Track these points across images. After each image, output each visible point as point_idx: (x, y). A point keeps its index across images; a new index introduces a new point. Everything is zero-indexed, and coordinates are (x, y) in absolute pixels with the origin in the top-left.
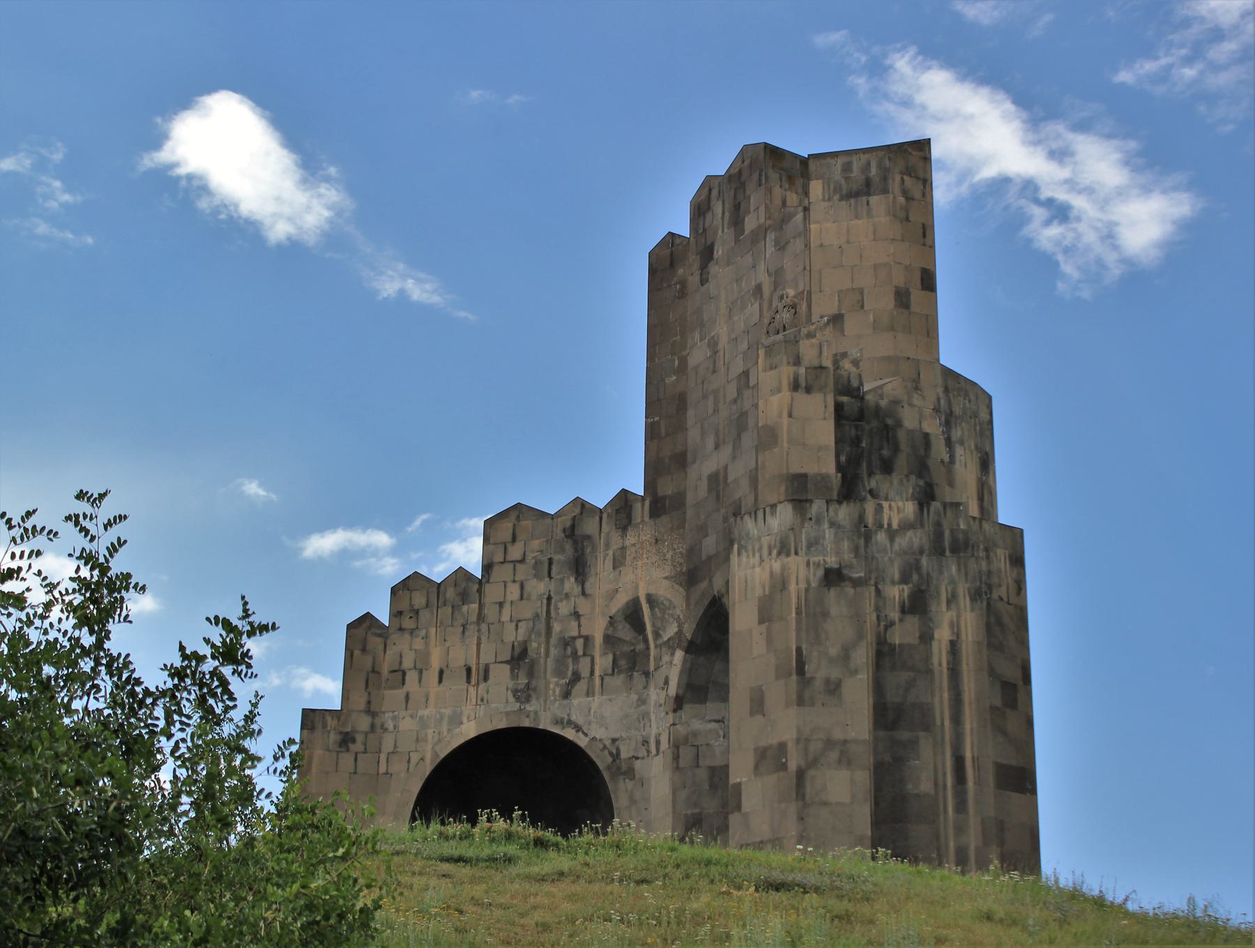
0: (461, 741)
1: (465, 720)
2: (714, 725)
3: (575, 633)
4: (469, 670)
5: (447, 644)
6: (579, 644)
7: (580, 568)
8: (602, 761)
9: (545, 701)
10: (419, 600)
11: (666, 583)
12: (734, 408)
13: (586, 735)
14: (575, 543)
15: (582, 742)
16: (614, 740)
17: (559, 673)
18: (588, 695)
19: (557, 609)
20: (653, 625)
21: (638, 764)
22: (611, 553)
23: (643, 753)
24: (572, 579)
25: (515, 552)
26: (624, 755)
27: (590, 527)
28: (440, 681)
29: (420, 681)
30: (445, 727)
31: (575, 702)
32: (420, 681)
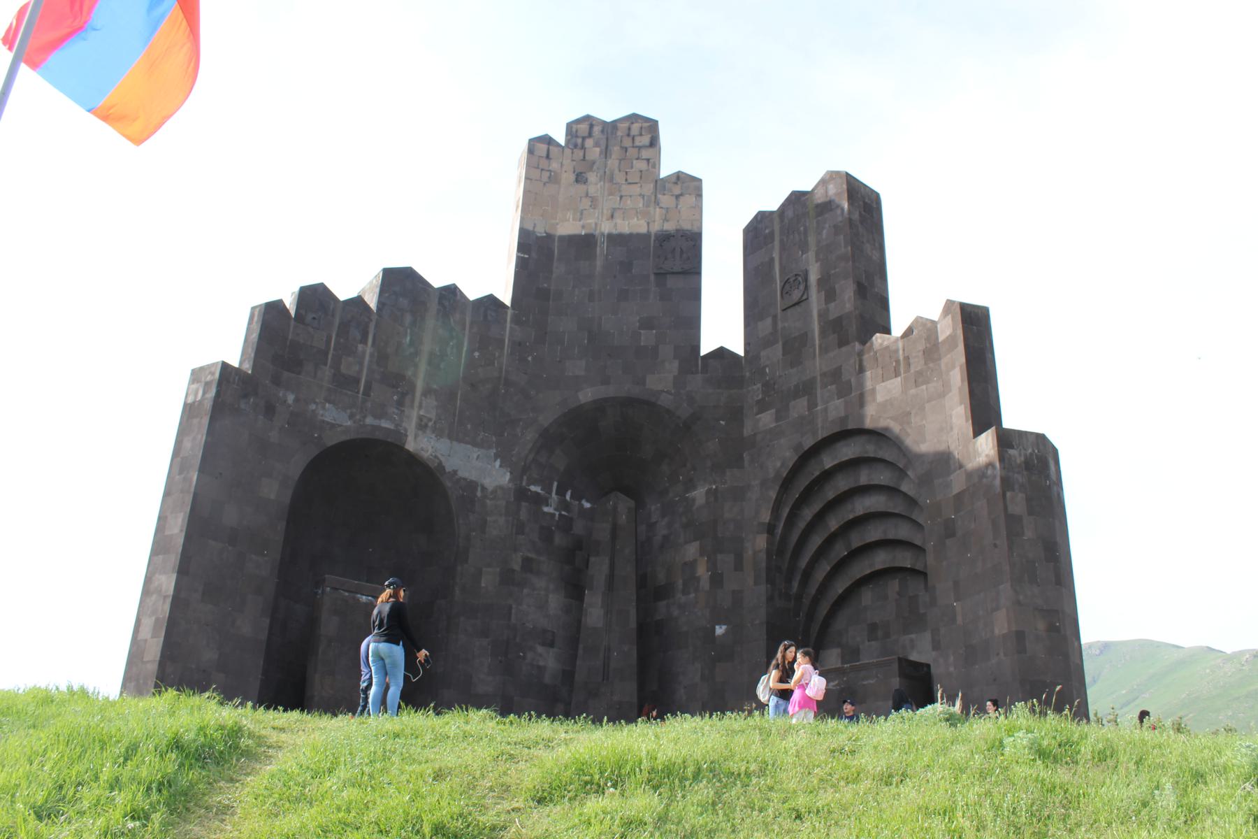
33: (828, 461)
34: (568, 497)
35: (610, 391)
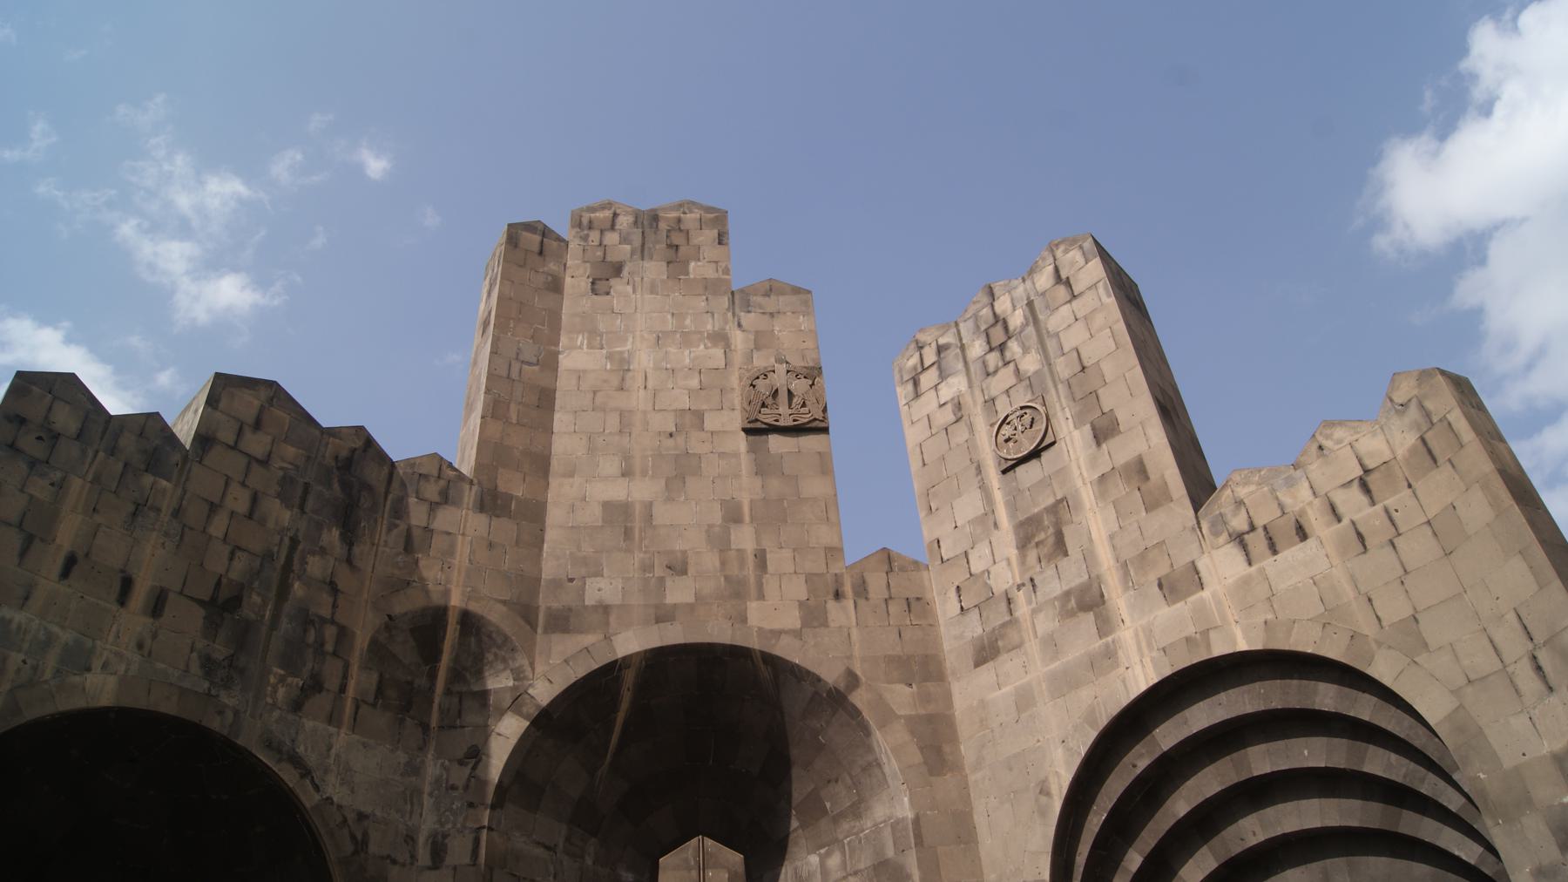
0: (78, 703)
1: (97, 664)
2: (539, 851)
3: (325, 612)
4: (127, 585)
5: (98, 518)
6: (330, 632)
7: (348, 520)
10: (65, 420)
11: (504, 609)
12: (670, 442)
13: (317, 788)
14: (345, 485)
15: (309, 799)
16: (361, 817)
17: (290, 663)
18: (330, 720)
19: (304, 562)
20: (456, 659)
21: (394, 871)
22: (403, 527)
24: (336, 533)
25: (257, 444)
26: (373, 848)
27: (374, 475)
28: (65, 573)
29: (23, 553)
30: (51, 660)
31: (309, 724)
32: (23, 553)
33: (1168, 735)
34: (589, 861)
35: (674, 635)
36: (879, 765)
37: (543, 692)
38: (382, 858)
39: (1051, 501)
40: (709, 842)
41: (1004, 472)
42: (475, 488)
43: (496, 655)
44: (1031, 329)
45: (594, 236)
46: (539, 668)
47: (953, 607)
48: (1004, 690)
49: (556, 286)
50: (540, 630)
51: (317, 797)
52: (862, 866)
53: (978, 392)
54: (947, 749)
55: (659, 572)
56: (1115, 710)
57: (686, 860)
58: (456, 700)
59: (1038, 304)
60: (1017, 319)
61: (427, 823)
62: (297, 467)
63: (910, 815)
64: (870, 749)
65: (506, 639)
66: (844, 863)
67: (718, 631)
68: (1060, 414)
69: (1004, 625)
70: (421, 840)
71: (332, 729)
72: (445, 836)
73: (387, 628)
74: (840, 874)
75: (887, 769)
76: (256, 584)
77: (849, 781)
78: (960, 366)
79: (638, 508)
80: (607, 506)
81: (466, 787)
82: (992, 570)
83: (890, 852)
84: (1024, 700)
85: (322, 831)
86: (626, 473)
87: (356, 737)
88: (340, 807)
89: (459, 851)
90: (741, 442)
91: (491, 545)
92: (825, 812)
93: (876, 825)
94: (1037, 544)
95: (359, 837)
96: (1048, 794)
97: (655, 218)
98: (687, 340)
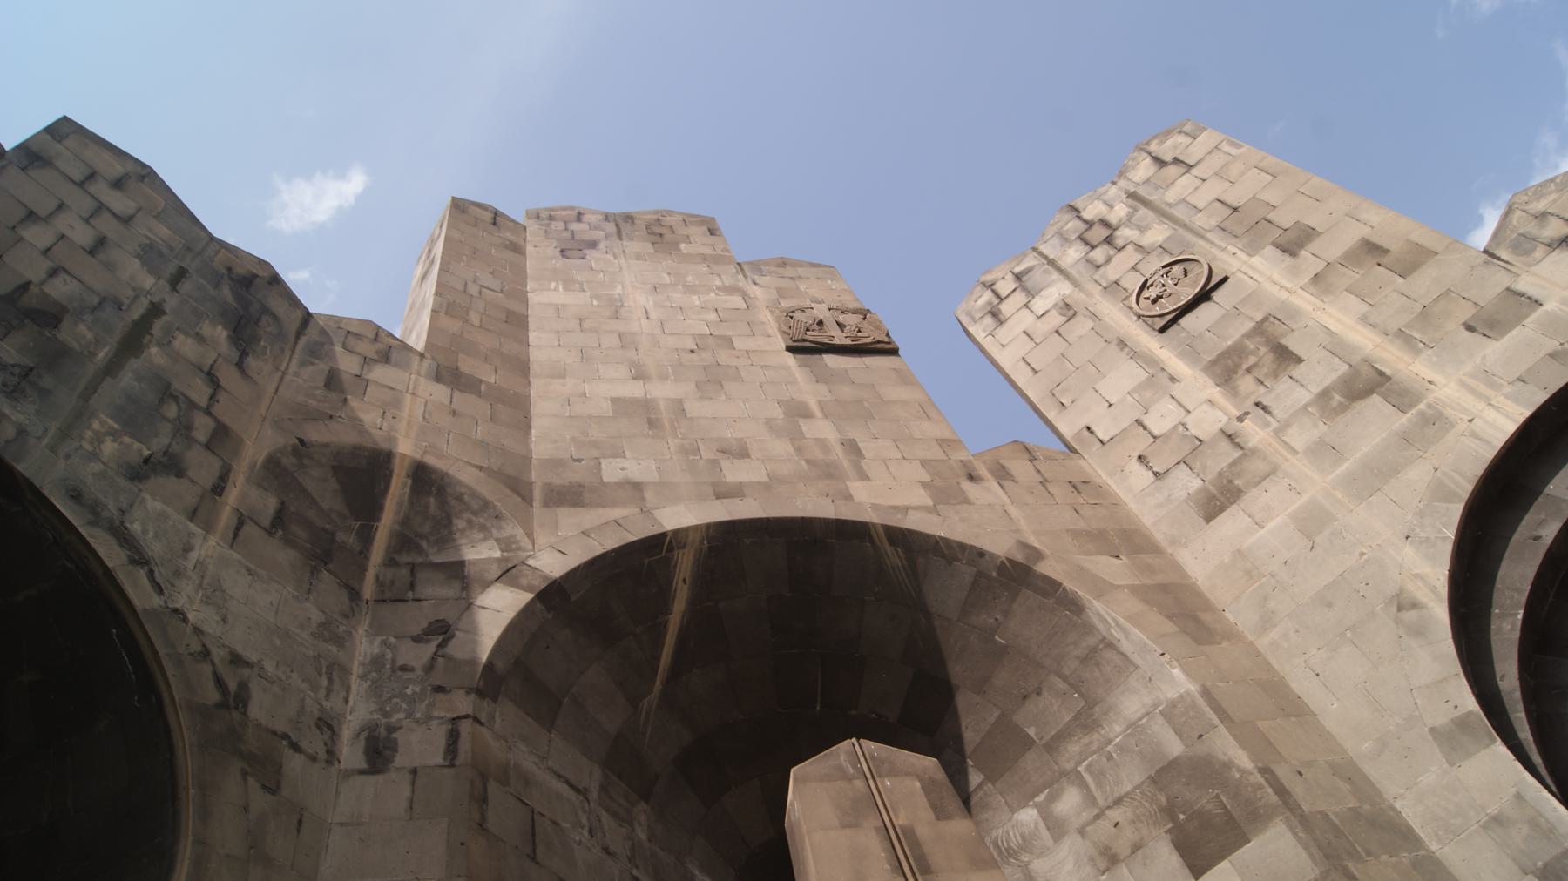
6: (202, 427)
8: (186, 689)
9: (65, 434)
13: (159, 590)
16: (236, 660)
17: (134, 418)
18: (193, 515)
20: (405, 522)
22: (323, 367)
23: (314, 742)
26: (256, 711)
34: (642, 834)
36: (1111, 646)
37: (552, 563)
38: (275, 733)
39: (1249, 325)
40: (871, 746)
41: (1162, 330)
42: (426, 363)
43: (470, 522)
44: (1143, 211)
45: (559, 225)
46: (542, 539)
47: (1140, 477)
48: (1270, 526)
49: (518, 249)
50: (536, 504)
51: (157, 601)
52: (1127, 787)
53: (1090, 286)
54: (1206, 617)
55: (706, 455)
56: (1479, 469)
57: (840, 768)
58: (405, 572)
59: (1142, 191)
60: (1120, 211)
61: (357, 711)
62: (171, 249)
63: (1193, 688)
64: (1088, 628)
65: (486, 504)
66: (1090, 799)
67: (811, 503)
68: (1220, 254)
69: (1234, 463)
70: (346, 734)
71: (192, 527)
72: (391, 729)
73: (295, 452)
74: (1086, 816)
75: (1125, 646)
76: (88, 317)
77: (1062, 685)
78: (1055, 275)
79: (662, 405)
80: (614, 401)
81: (430, 668)
82: (1189, 420)
83: (1174, 747)
84: (1312, 523)
85: (162, 652)
86: (640, 375)
87: (236, 556)
88: (197, 631)
89: (421, 745)
90: (791, 360)
91: (454, 413)
92: (1028, 743)
93: (1133, 725)
94: (1249, 371)
95: (232, 686)
96: (1415, 605)
97: (629, 218)
98: (691, 289)
